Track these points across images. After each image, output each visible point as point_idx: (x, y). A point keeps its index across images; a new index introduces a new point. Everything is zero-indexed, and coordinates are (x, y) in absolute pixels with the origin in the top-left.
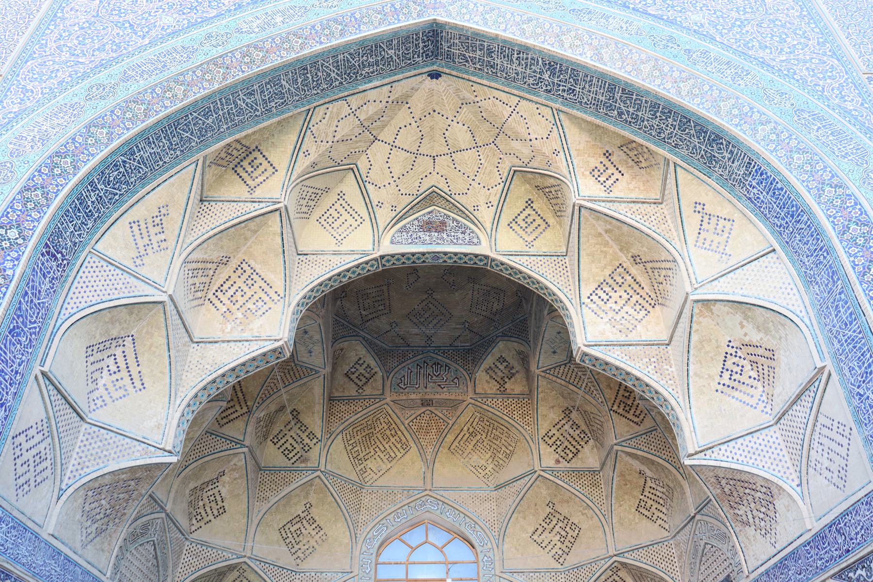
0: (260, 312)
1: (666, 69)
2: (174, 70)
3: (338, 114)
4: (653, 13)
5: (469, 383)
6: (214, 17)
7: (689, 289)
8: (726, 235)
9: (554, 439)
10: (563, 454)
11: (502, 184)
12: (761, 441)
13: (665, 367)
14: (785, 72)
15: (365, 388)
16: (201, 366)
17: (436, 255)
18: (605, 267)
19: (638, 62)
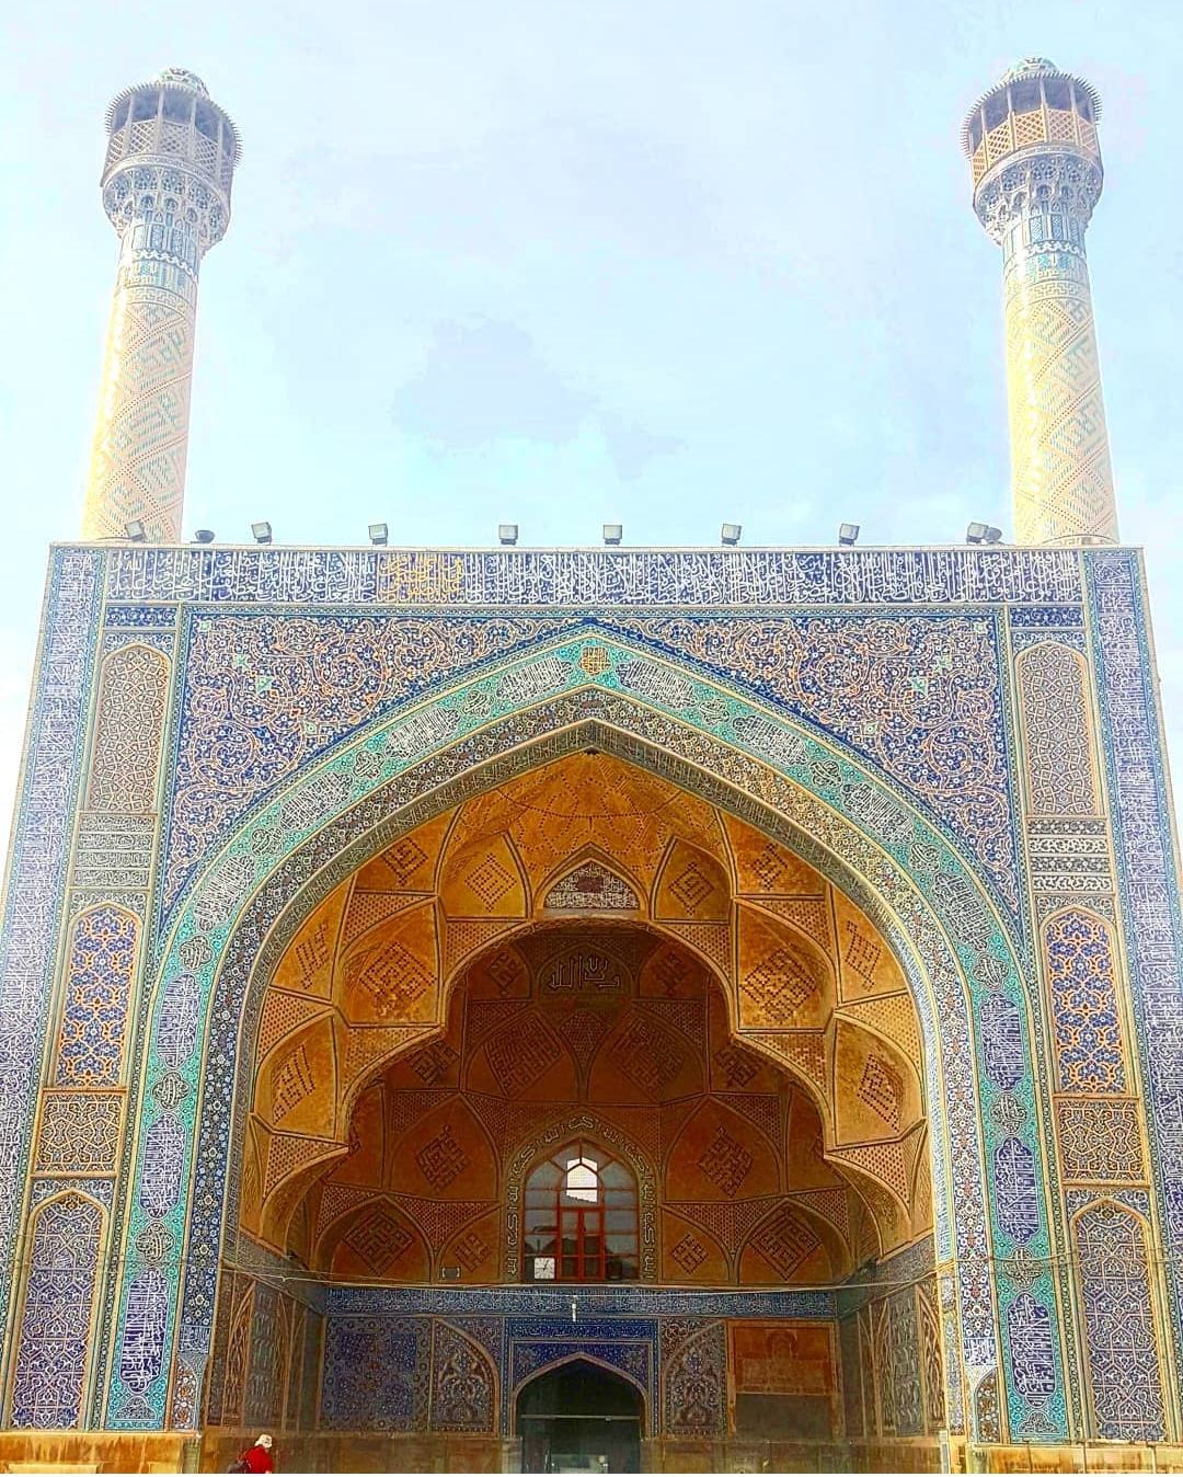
0: (415, 994)
1: (821, 813)
2: (335, 811)
3: (489, 801)
4: (824, 722)
5: (632, 983)
6: (361, 725)
7: (835, 1006)
8: (872, 962)
9: (728, 1057)
10: (737, 1076)
11: (663, 849)
12: (887, 1153)
13: (817, 1058)
14: (944, 817)
15: (508, 988)
16: (361, 1055)
17: (591, 920)
18: (765, 951)
19: (795, 800)
